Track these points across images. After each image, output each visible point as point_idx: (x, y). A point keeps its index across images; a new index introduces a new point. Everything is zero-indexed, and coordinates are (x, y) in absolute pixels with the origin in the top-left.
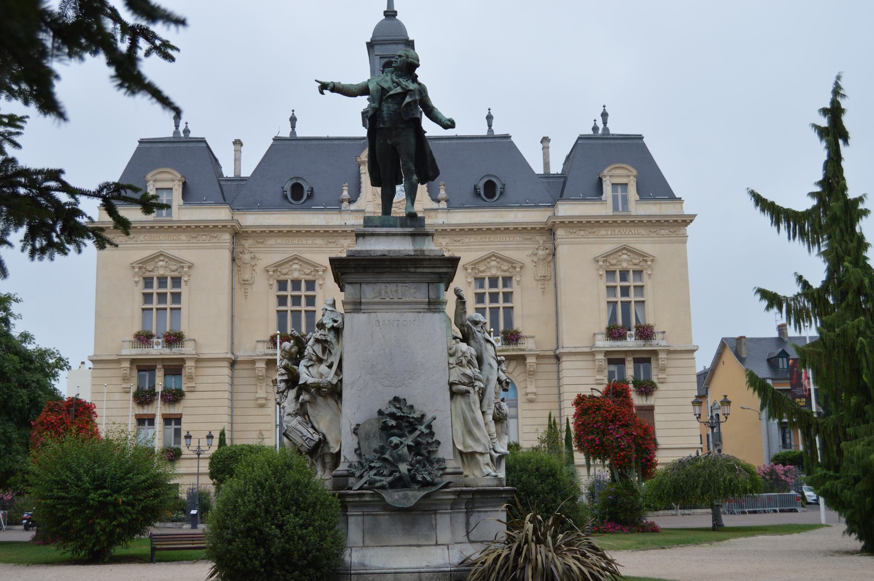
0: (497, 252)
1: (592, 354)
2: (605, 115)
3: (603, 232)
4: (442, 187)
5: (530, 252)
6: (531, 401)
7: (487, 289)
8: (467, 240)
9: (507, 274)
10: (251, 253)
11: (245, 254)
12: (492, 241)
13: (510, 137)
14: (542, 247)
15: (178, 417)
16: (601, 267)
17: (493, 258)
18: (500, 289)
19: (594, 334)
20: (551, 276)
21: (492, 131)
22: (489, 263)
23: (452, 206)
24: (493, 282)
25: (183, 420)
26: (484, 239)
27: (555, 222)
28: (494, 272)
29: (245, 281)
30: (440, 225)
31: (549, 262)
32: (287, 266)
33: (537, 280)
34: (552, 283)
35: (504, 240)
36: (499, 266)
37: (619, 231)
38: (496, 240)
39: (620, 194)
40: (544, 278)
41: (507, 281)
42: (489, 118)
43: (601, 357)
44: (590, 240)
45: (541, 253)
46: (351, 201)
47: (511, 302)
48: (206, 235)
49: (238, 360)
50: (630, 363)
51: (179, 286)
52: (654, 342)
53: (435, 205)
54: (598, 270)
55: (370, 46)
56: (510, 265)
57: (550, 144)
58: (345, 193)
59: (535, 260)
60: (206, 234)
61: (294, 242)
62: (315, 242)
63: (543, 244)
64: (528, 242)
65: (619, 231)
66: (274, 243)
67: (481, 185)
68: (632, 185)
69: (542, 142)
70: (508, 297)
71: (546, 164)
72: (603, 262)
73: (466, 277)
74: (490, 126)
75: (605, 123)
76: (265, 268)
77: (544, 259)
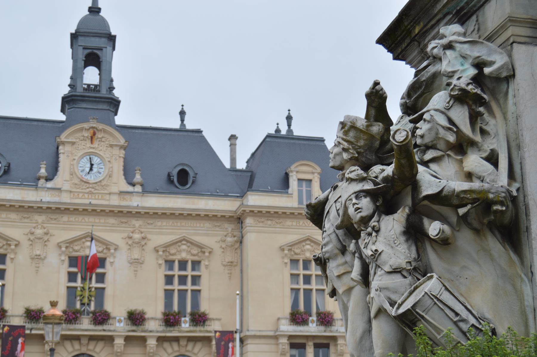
1: (276, 337)
2: (289, 118)
3: (288, 223)
4: (138, 171)
5: (219, 238)
7: (176, 272)
8: (159, 224)
9: (196, 258)
12: (183, 226)
13: (202, 132)
14: (230, 235)
16: (286, 255)
17: (184, 242)
18: (189, 272)
19: (279, 319)
20: (237, 262)
21: (184, 126)
22: (179, 246)
23: (146, 191)
24: (183, 265)
26: (176, 224)
27: (244, 211)
28: (184, 255)
30: (134, 208)
31: (236, 249)
33: (224, 266)
34: (238, 269)
35: (195, 225)
36: (189, 249)
37: (304, 223)
38: (187, 225)
39: (304, 189)
40: (231, 264)
41: (196, 264)
42: (182, 113)
43: (284, 341)
44: (277, 229)
45: (229, 239)
46: (48, 179)
47: (199, 285)
50: (310, 348)
52: (334, 328)
53: (130, 189)
54: (283, 258)
55: (74, 37)
56: (200, 250)
57: (238, 142)
58: (43, 171)
59: (224, 246)
62: (9, 216)
63: (232, 231)
64: (217, 229)
65: (304, 223)
67: (175, 173)
68: (316, 182)
69: (229, 139)
70: (196, 280)
71: (233, 160)
72: (288, 251)
73: (157, 259)
74: (182, 120)
75: (289, 125)
77: (232, 246)
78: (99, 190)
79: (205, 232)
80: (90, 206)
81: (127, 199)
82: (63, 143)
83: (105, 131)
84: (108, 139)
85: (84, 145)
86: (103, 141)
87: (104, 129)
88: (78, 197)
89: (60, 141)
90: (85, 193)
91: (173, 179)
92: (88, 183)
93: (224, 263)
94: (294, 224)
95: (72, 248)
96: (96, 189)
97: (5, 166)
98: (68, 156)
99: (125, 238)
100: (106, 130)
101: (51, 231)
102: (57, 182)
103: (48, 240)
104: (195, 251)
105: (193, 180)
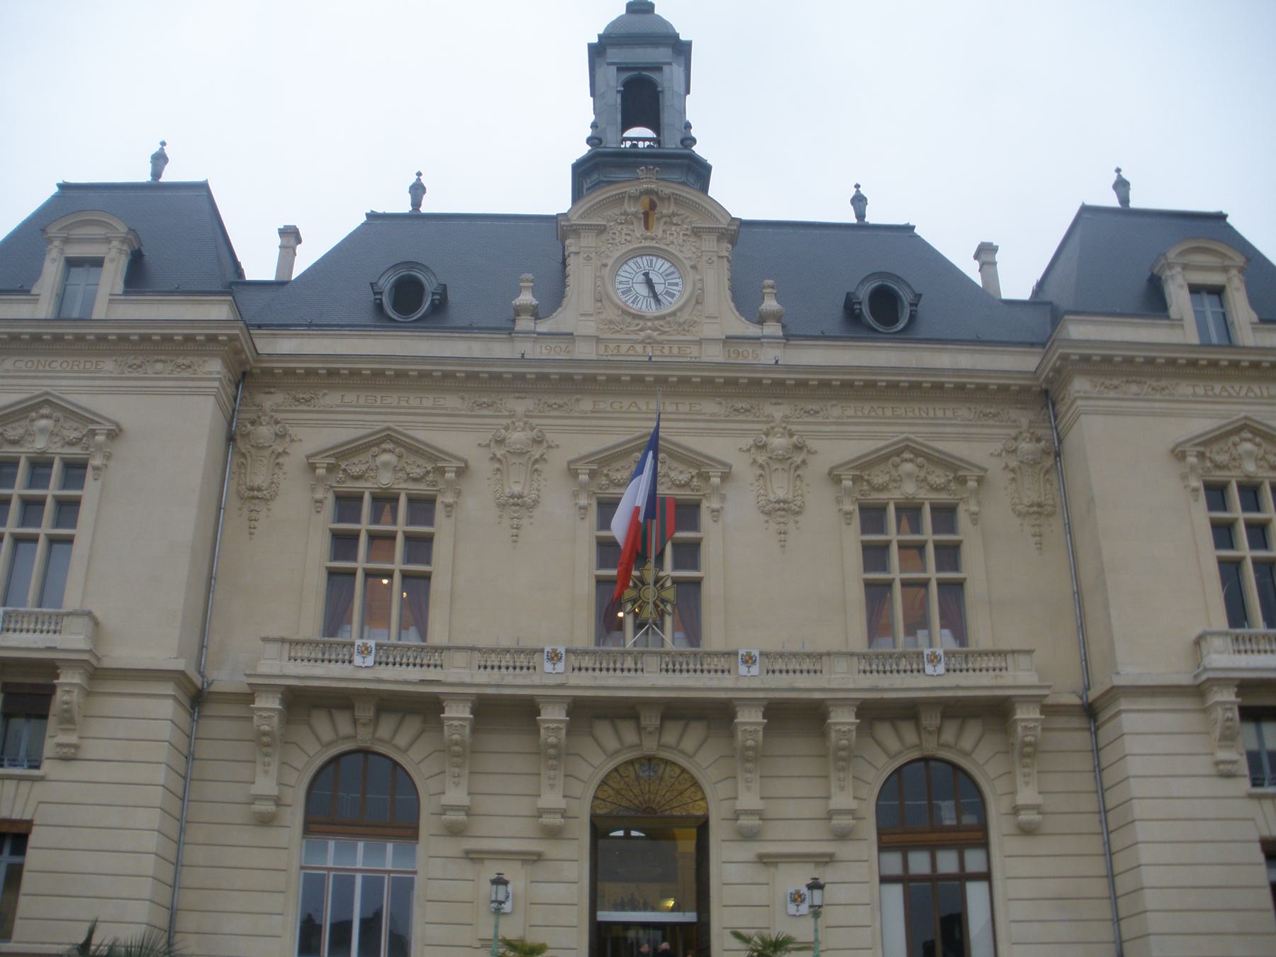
0: (920, 440)
1: (1198, 691)
3: (1185, 389)
4: (769, 290)
5: (998, 446)
6: (1027, 831)
7: (893, 534)
8: (836, 412)
10: (277, 422)
11: (261, 424)
15: (21, 830)
16: (1193, 468)
17: (907, 455)
19: (1198, 641)
20: (1054, 506)
22: (896, 466)
25: (33, 840)
26: (880, 412)
27: (1065, 358)
29: (252, 489)
30: (766, 368)
31: (1047, 472)
32: (364, 457)
33: (1020, 514)
35: (931, 414)
36: (922, 474)
37: (1224, 389)
38: (910, 414)
40: (1038, 511)
43: (1228, 696)
44: (1157, 405)
45: (1025, 446)
48: (164, 362)
49: (213, 689)
51: (80, 483)
53: (753, 330)
54: (1184, 477)
55: (597, 52)
60: (163, 358)
61: (389, 401)
62: (442, 402)
63: (1030, 427)
64: (991, 422)
65: (1224, 389)
66: (338, 402)
68: (1238, 289)
70: (949, 555)
72: (1197, 456)
73: (839, 501)
76: (308, 457)
77: (1036, 463)
78: (670, 335)
79: (960, 430)
80: (648, 369)
81: (745, 353)
82: (575, 230)
83: (678, 200)
84: (687, 217)
85: (626, 234)
86: (675, 222)
87: (676, 194)
88: (618, 351)
89: (567, 226)
90: (636, 342)
91: (861, 309)
92: (641, 317)
93: (1019, 507)
94: (1200, 391)
95: (607, 475)
96: (664, 333)
97: (434, 294)
98: (588, 258)
99: (749, 450)
100: (680, 196)
101: (549, 436)
102: (563, 320)
103: (542, 459)
104: (938, 478)
105: (911, 311)
